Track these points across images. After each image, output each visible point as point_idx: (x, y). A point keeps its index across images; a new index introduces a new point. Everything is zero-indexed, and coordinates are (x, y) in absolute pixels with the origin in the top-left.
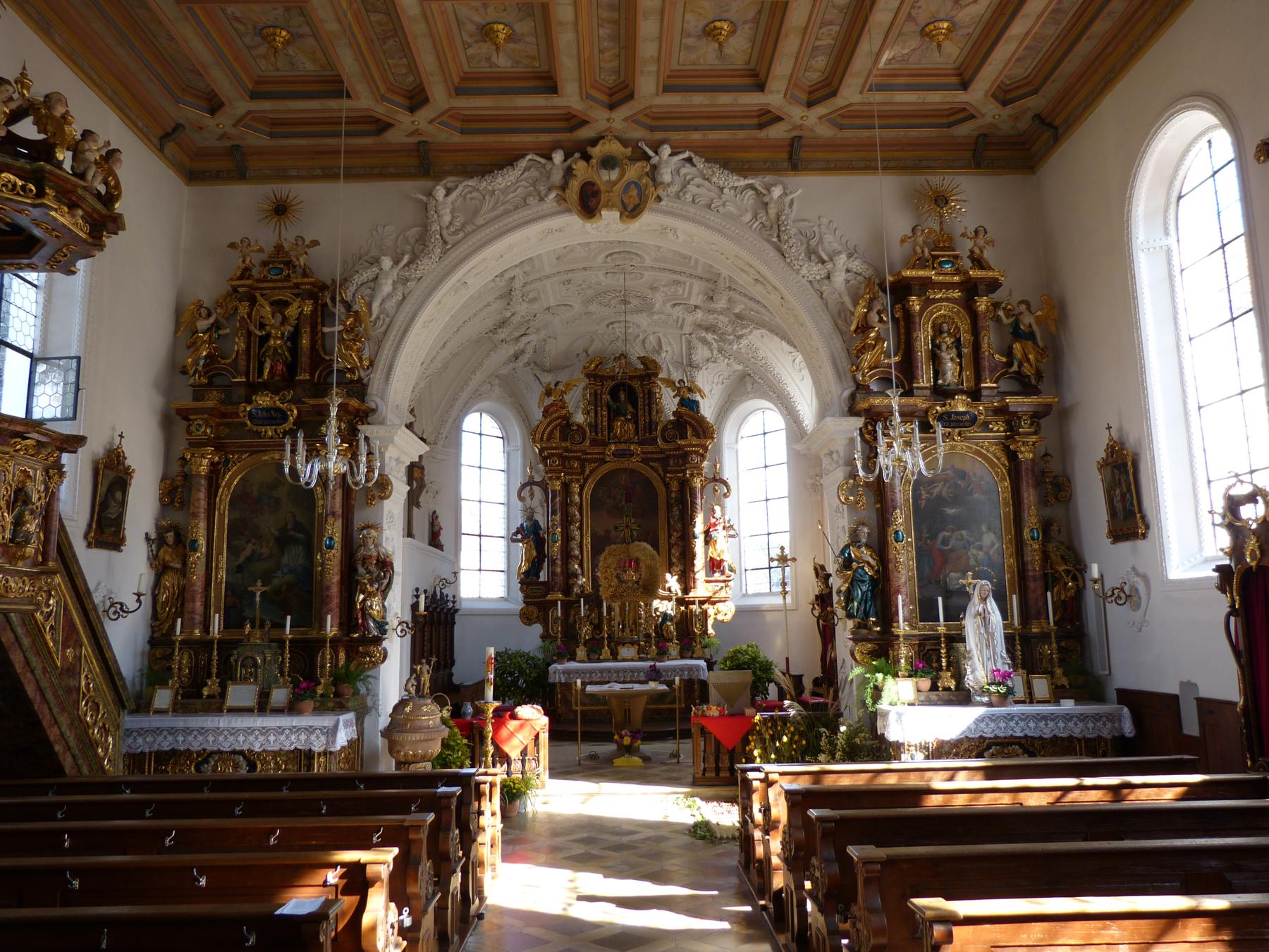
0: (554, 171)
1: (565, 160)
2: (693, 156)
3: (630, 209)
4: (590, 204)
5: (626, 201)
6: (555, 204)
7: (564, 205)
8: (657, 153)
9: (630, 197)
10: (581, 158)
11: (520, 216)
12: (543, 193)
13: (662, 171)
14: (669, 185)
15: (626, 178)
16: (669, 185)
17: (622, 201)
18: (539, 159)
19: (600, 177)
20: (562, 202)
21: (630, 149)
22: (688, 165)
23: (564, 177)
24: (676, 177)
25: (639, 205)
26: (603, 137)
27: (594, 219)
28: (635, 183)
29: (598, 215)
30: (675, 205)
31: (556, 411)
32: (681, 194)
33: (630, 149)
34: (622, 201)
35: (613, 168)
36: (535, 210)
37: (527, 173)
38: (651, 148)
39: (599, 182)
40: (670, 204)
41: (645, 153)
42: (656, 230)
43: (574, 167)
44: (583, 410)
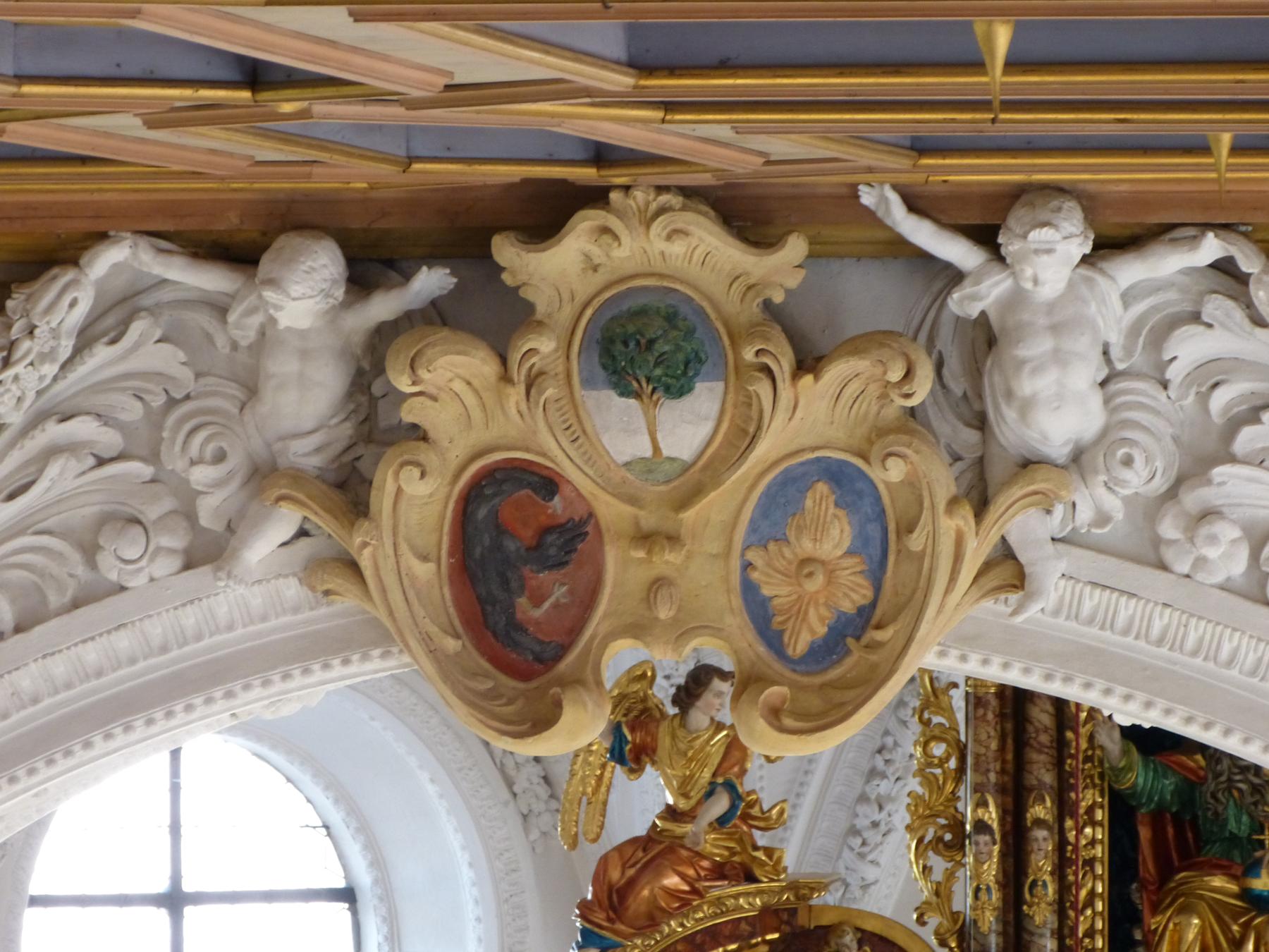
3: (800, 644)
5: (775, 589)
6: (292, 589)
7: (348, 602)
11: (59, 667)
12: (209, 511)
13: (1027, 386)
15: (765, 449)
17: (749, 590)
19: (578, 431)
22: (1218, 307)
30: (1126, 609)
31: (683, 902)
32: (1169, 529)
33: (795, 248)
34: (749, 590)
35: (678, 387)
36: (156, 629)
37: (102, 353)
40: (1092, 600)
44: (922, 813)
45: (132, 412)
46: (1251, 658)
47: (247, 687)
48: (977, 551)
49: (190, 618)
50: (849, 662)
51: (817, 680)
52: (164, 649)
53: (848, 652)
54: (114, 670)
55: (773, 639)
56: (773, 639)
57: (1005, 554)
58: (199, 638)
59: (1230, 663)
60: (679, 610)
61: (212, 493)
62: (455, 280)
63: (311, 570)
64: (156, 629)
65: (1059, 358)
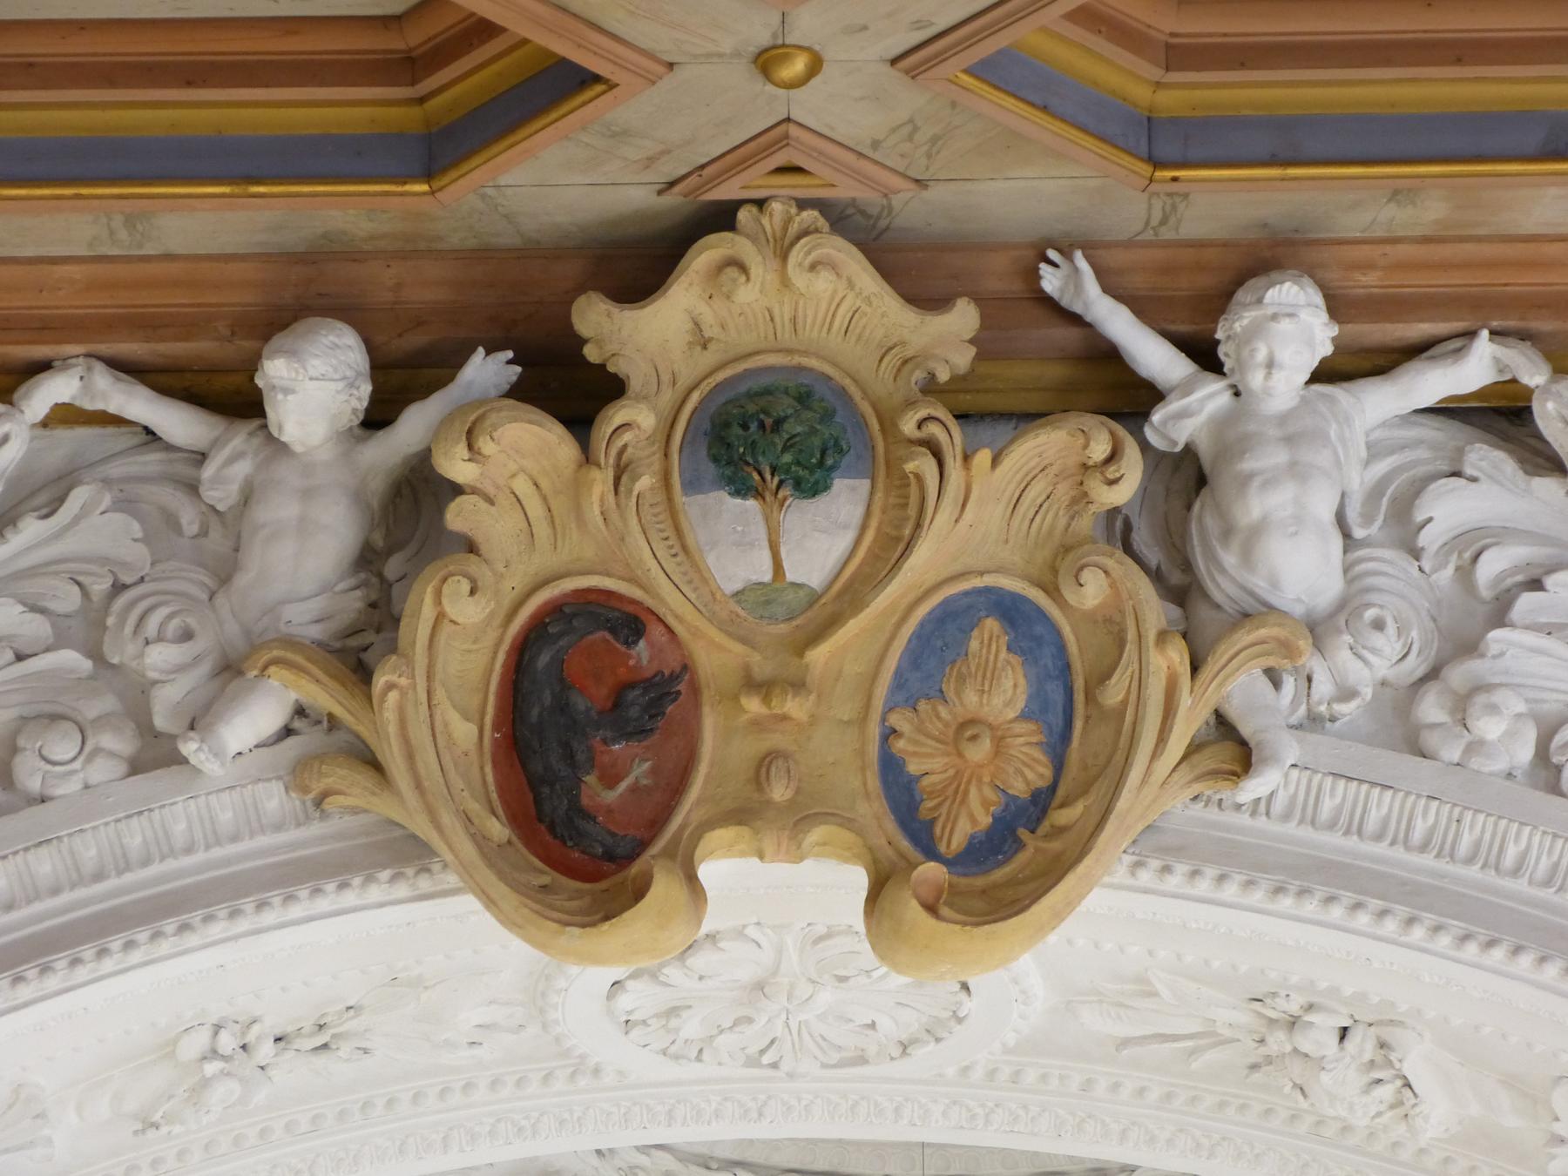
0: (279, 510)
1: (377, 418)
2: (1533, 373)
3: (957, 835)
4: (600, 795)
6: (274, 798)
8: (1205, 356)
9: (968, 727)
10: (518, 392)
12: (165, 708)
13: (1256, 506)
14: (1318, 629)
15: (924, 561)
16: (1318, 629)
17: (891, 766)
18: (139, 405)
20: (352, 784)
21: (963, 318)
22: (1486, 457)
23: (367, 559)
24: (1386, 563)
25: (1041, 802)
26: (721, 218)
27: (635, 924)
28: (1010, 610)
29: (664, 887)
30: (1380, 806)
32: (1431, 709)
33: (963, 318)
34: (891, 766)
35: (811, 483)
38: (1143, 308)
39: (672, 602)
40: (1334, 797)
41: (1108, 355)
42: (1211, 1038)
43: (456, 466)
45: (67, 599)
46: (1544, 864)
47: (208, 919)
48: (1190, 722)
49: (135, 836)
50: (1022, 858)
51: (980, 882)
52: (99, 876)
53: (1020, 845)
54: (29, 902)
55: (924, 839)
56: (924, 839)
57: (1223, 726)
58: (146, 862)
59: (1516, 872)
60: (798, 791)
61: (174, 680)
62: (519, 369)
63: (298, 775)
64: (89, 851)
65: (1296, 471)
